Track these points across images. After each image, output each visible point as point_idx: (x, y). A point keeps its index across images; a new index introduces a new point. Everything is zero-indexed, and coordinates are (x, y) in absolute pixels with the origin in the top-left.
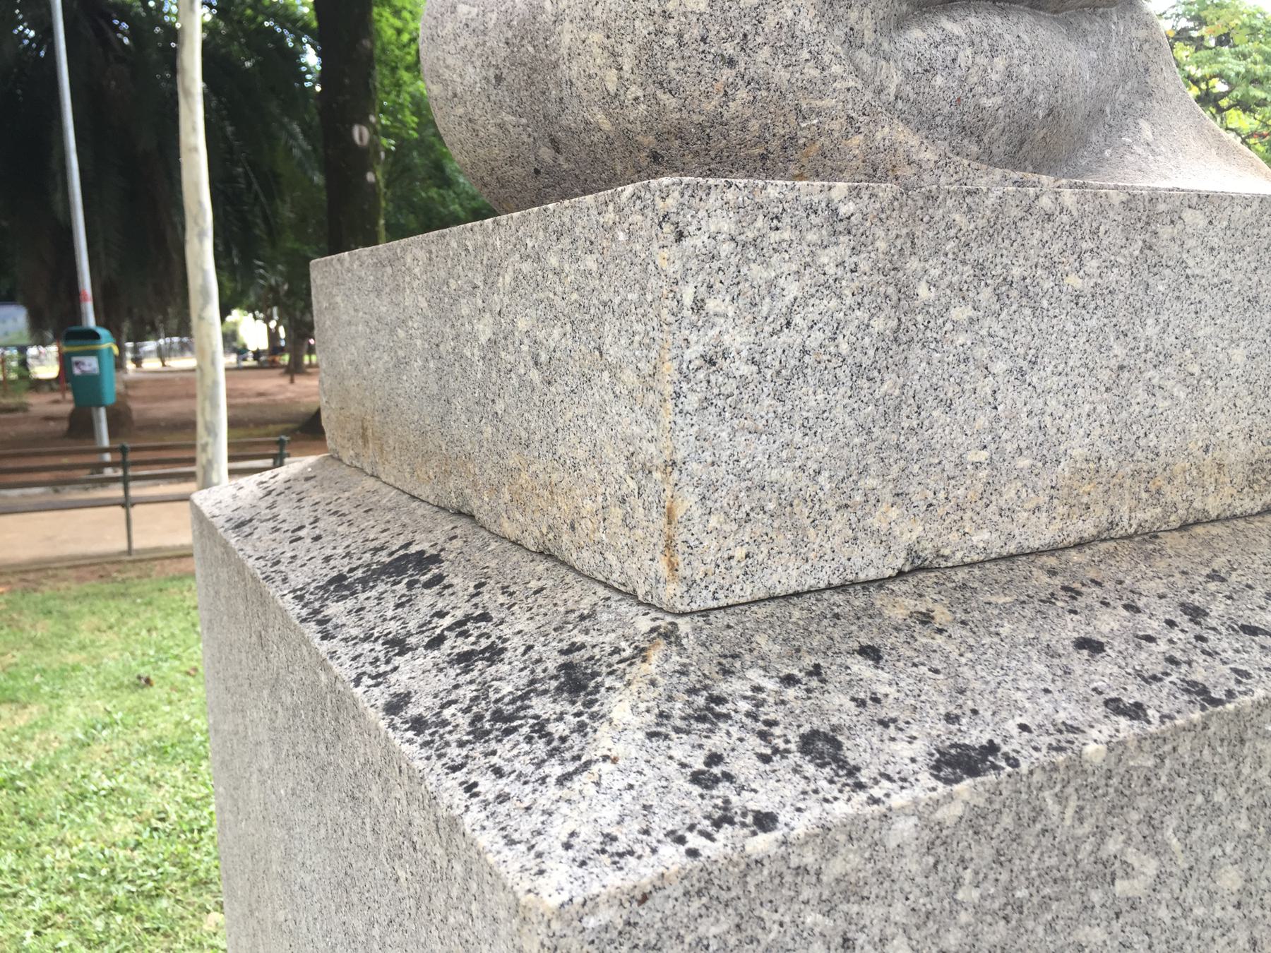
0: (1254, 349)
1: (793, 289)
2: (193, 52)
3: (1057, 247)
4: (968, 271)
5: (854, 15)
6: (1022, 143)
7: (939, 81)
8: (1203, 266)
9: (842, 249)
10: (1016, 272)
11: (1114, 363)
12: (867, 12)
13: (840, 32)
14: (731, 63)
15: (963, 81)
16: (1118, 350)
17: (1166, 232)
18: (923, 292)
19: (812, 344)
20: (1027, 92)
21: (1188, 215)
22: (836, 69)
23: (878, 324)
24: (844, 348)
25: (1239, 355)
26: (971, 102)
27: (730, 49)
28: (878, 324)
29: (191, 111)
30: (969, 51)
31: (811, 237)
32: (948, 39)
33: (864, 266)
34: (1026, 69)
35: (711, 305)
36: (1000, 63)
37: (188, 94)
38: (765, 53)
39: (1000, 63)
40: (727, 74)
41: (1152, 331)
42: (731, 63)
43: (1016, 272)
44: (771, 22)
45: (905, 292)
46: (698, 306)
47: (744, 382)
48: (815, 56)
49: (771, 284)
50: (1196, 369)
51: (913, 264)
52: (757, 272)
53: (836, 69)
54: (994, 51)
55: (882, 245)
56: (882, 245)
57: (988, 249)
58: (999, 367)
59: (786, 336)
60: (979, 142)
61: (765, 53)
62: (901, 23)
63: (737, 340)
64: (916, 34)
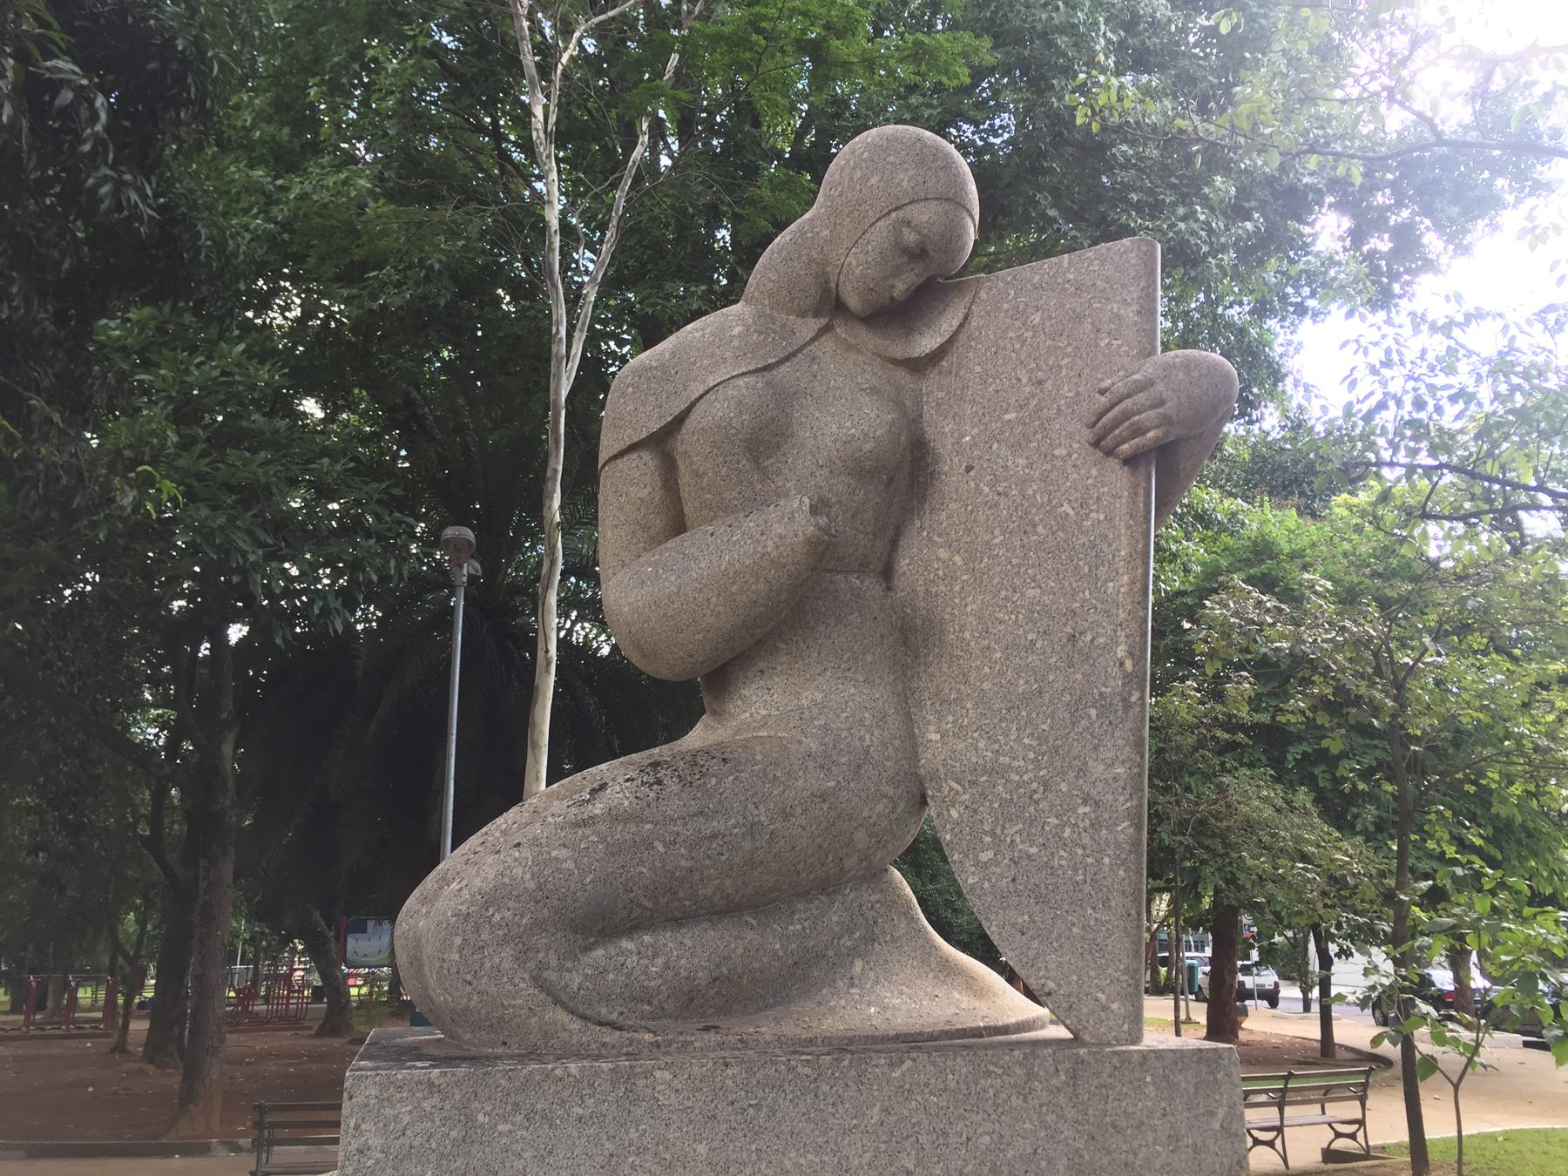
0: (716, 1144)
1: (407, 1119)
2: (544, 707)
3: (566, 1094)
4: (509, 1107)
5: (541, 956)
6: (691, 1000)
7: (611, 976)
8: (666, 1098)
9: (435, 1100)
10: (539, 1106)
11: (607, 1153)
12: (552, 952)
13: (531, 965)
14: (470, 983)
15: (629, 975)
16: (608, 1145)
17: (641, 1083)
18: (481, 1117)
19: (415, 1143)
20: (684, 974)
21: (658, 1074)
22: (522, 985)
23: (454, 1134)
24: (434, 1145)
25: (702, 1148)
26: (637, 986)
27: (469, 977)
28: (454, 1134)
29: (537, 762)
30: (635, 958)
31: (419, 1095)
32: (621, 953)
33: (447, 1107)
34: (683, 962)
35: (364, 1127)
36: (660, 961)
37: (536, 746)
38: (485, 979)
39: (660, 961)
40: (469, 988)
41: (633, 1135)
42: (470, 983)
43: (539, 1106)
44: (488, 965)
45: (471, 1119)
46: (357, 1127)
47: (378, 1161)
48: (511, 980)
49: (396, 1116)
50: (668, 1156)
51: (476, 1105)
52: (389, 1112)
53: (522, 985)
54: (655, 955)
55: (458, 1097)
56: (458, 1097)
57: (520, 1098)
58: (527, 1155)
59: (401, 1141)
60: (650, 1003)
61: (485, 979)
62: (587, 949)
63: (376, 1142)
64: (600, 952)
